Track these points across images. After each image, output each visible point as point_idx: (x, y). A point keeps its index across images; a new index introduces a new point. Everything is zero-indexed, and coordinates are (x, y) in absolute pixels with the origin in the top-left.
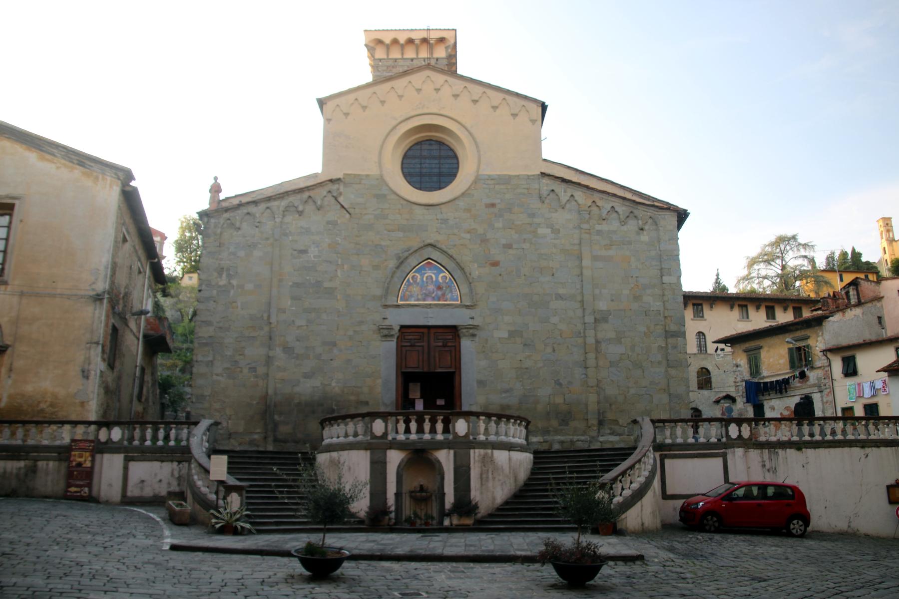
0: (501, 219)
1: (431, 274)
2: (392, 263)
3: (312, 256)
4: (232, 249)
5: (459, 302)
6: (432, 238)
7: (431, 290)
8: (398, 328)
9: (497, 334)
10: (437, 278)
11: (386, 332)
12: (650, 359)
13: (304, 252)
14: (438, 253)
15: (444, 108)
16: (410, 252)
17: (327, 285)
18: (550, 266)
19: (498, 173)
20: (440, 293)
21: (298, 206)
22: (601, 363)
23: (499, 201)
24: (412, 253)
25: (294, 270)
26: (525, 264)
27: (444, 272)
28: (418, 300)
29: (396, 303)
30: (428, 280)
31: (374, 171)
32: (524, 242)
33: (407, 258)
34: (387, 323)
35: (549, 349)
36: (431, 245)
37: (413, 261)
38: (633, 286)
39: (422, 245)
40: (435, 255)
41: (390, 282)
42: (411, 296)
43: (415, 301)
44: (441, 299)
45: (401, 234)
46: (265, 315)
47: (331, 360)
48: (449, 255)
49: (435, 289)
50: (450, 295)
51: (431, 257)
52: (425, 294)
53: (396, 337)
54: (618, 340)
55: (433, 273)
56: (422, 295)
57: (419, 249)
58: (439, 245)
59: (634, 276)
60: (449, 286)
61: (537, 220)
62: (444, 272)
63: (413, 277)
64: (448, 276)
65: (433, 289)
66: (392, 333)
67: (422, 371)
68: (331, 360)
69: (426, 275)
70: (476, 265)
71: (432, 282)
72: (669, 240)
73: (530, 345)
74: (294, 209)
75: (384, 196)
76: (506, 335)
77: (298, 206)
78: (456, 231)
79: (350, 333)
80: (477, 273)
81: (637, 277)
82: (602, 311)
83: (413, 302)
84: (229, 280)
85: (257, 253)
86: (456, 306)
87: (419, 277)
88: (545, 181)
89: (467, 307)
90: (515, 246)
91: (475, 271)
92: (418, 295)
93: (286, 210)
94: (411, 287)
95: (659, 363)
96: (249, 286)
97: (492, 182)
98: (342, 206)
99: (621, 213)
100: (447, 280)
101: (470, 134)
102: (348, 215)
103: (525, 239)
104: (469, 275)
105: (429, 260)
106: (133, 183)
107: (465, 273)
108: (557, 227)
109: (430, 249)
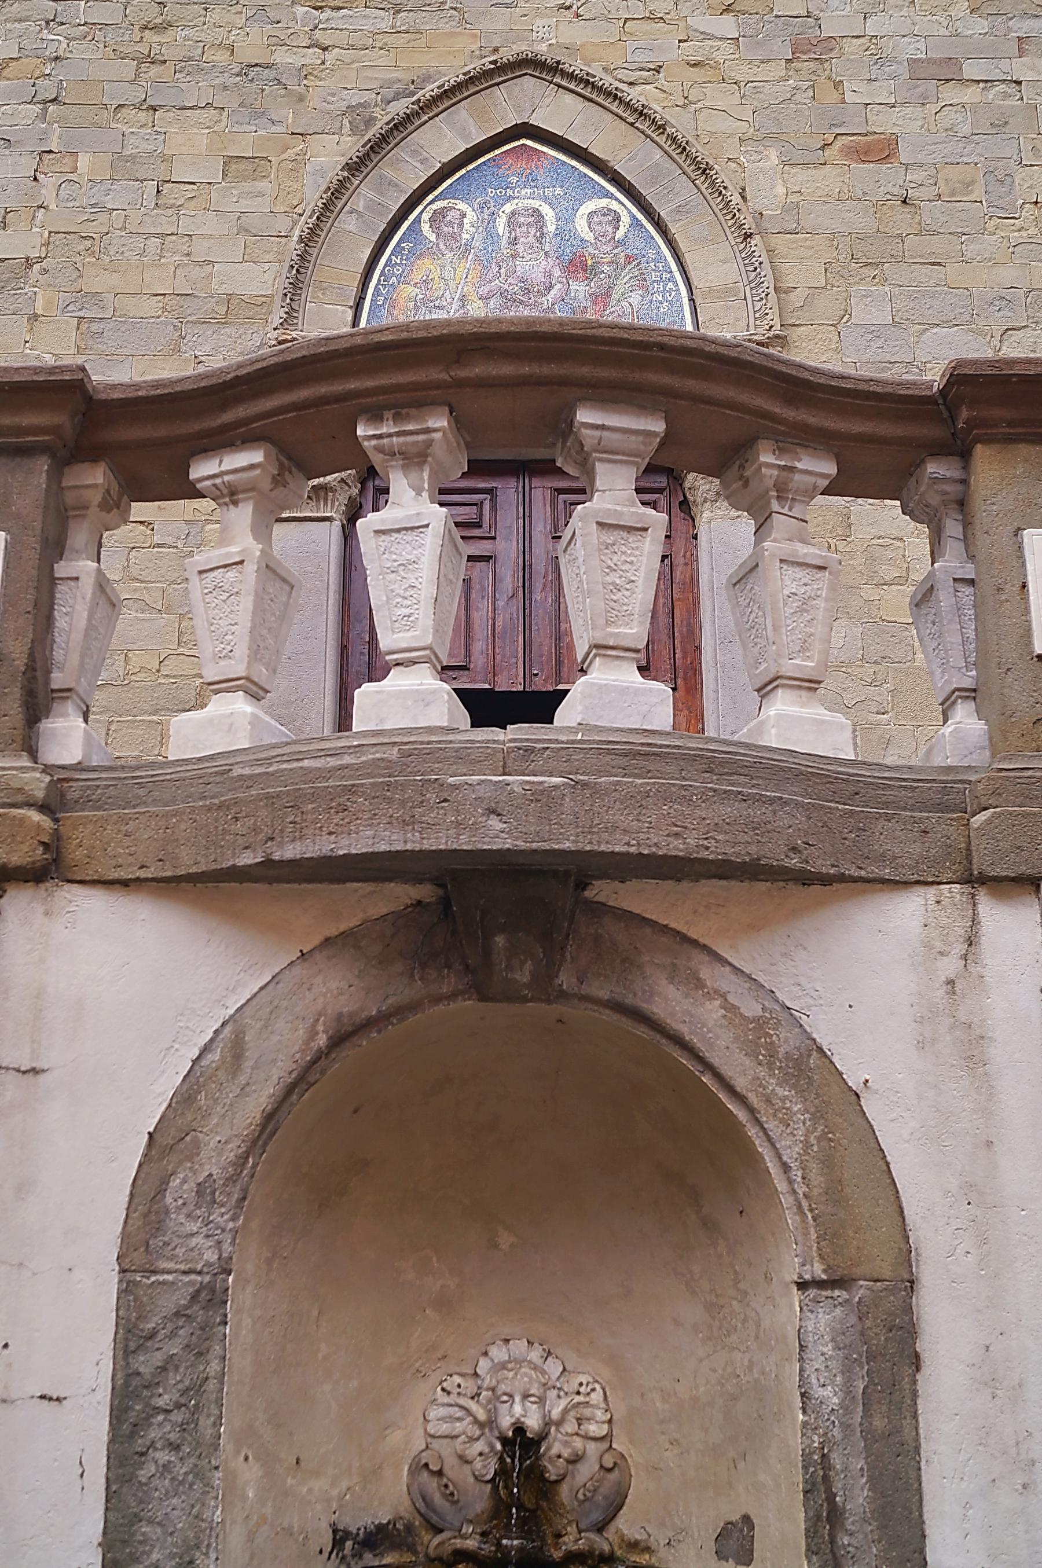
1: (535, 204)
5: (689, 327)
7: (538, 276)
10: (566, 220)
14: (569, 99)
24: (435, 100)
27: (611, 196)
33: (402, 125)
39: (486, 63)
41: (313, 231)
48: (628, 105)
49: (557, 273)
50: (635, 298)
53: (343, 499)
55: (545, 199)
56: (485, 298)
57: (471, 80)
58: (576, 65)
63: (438, 217)
64: (625, 209)
67: (487, 686)
69: (508, 208)
71: (541, 237)
80: (781, 190)
87: (471, 215)
90: (971, 70)
94: (427, 263)
100: (620, 234)
104: (736, 199)
109: (528, 85)
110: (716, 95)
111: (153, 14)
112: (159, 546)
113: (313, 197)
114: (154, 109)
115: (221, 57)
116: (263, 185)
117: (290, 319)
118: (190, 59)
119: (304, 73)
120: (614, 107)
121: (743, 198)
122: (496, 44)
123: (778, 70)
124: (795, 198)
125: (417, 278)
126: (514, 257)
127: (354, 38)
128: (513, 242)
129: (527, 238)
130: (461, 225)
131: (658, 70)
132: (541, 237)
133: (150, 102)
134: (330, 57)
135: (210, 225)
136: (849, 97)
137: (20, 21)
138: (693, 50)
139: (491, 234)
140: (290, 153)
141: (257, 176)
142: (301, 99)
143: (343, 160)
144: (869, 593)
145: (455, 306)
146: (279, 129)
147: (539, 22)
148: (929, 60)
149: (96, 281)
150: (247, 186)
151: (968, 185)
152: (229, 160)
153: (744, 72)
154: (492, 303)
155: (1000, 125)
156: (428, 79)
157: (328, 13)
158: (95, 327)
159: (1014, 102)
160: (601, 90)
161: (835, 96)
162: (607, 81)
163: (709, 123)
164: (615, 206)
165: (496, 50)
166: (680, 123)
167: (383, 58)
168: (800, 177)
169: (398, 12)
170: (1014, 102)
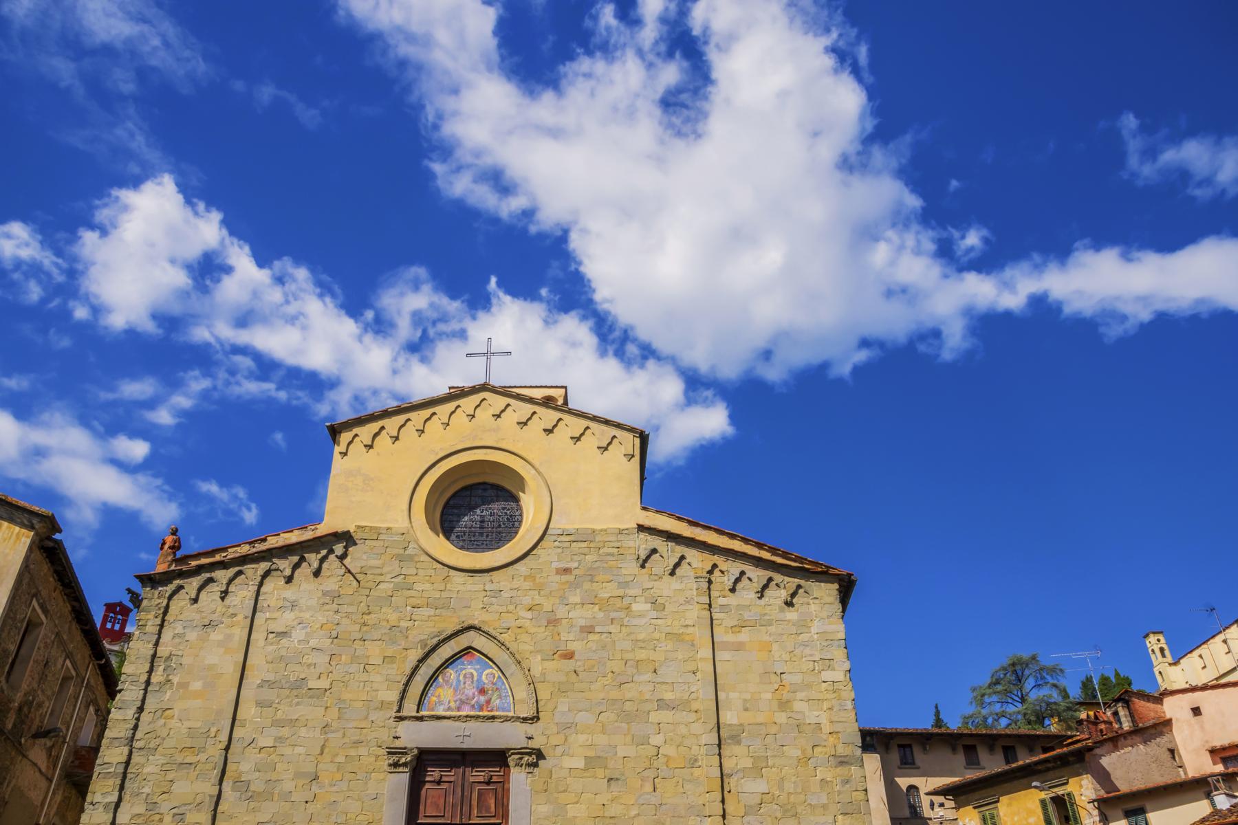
0: (578, 591)
1: (472, 671)
2: (415, 655)
3: (296, 641)
4: (179, 630)
6: (477, 618)
7: (471, 694)
8: (416, 752)
9: (568, 763)
10: (480, 676)
11: (394, 758)
12: (809, 801)
13: (283, 634)
15: (503, 439)
16: (442, 637)
17: (311, 684)
18: (651, 658)
19: (577, 526)
20: (483, 699)
21: (284, 569)
22: (730, 808)
23: (576, 565)
25: (267, 663)
26: (613, 654)
28: (449, 709)
29: (414, 714)
30: (467, 680)
31: (399, 521)
32: (612, 623)
34: (398, 744)
35: (648, 787)
36: (471, 628)
37: (446, 651)
38: (776, 686)
40: (479, 641)
42: (440, 703)
43: (444, 710)
44: (485, 708)
45: (432, 612)
46: (213, 730)
47: (307, 802)
48: (499, 641)
49: (476, 693)
51: (473, 645)
52: (461, 700)
54: (757, 770)
55: (475, 669)
56: (455, 701)
58: (485, 628)
59: (778, 673)
60: (497, 689)
61: (631, 592)
62: (492, 668)
65: (474, 694)
66: (403, 760)
67: (449, 822)
68: (307, 802)
69: (464, 672)
70: (539, 657)
71: (472, 682)
72: (829, 617)
73: (617, 779)
74: (279, 572)
75: (411, 558)
76: (580, 764)
77: (284, 569)
78: (511, 608)
79: (341, 759)
80: (541, 668)
81: (781, 674)
82: (730, 725)
83: (441, 713)
84: (168, 675)
85: (216, 636)
86: (507, 719)
88: (642, 535)
89: (525, 720)
90: (598, 629)
91: (537, 666)
92: (449, 703)
93: (267, 574)
94: (440, 690)
95: (824, 807)
96: (197, 685)
97: (568, 538)
98: (349, 571)
99: (755, 580)
101: (539, 473)
102: (355, 582)
103: (612, 619)
105: (470, 650)
106: (57, 536)
107: (522, 669)
108: (660, 600)
109: (472, 633)
110: (524, 637)
111: (365, 610)
112: (358, 780)
113: (408, 671)
114: (364, 640)
115: (385, 623)
116: (394, 666)
117: (399, 711)
118: (376, 624)
119: (408, 629)
120: (495, 641)
121: (529, 670)
122: (464, 619)
123: (543, 629)
124: (544, 671)
125: (437, 694)
126: (464, 688)
127: (423, 618)
128: (465, 683)
129: (468, 682)
130: (450, 677)
131: (509, 629)
132: (472, 682)
133: (364, 638)
134: (416, 623)
135: (378, 678)
136: (563, 638)
137: (328, 611)
138: (519, 623)
139: (459, 681)
140: (403, 655)
141: (393, 663)
142: (407, 637)
143: (417, 658)
144: (556, 795)
145: (447, 703)
146: (399, 647)
147: (476, 613)
148: (586, 626)
149: (346, 696)
150: (389, 666)
151: (593, 666)
152: (385, 657)
153: (532, 630)
154: (457, 703)
155: (604, 647)
156: (443, 631)
157: (415, 610)
158: (344, 710)
159: (609, 639)
160: (492, 636)
161: (558, 638)
162: (493, 633)
163: (522, 647)
164: (494, 671)
165: (463, 622)
166: (513, 647)
167: (431, 624)
168: (547, 664)
169: (436, 609)
170: (609, 639)
